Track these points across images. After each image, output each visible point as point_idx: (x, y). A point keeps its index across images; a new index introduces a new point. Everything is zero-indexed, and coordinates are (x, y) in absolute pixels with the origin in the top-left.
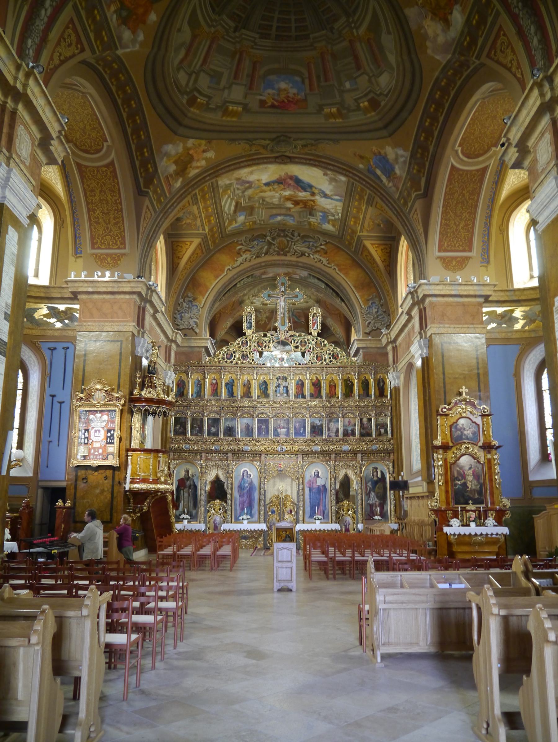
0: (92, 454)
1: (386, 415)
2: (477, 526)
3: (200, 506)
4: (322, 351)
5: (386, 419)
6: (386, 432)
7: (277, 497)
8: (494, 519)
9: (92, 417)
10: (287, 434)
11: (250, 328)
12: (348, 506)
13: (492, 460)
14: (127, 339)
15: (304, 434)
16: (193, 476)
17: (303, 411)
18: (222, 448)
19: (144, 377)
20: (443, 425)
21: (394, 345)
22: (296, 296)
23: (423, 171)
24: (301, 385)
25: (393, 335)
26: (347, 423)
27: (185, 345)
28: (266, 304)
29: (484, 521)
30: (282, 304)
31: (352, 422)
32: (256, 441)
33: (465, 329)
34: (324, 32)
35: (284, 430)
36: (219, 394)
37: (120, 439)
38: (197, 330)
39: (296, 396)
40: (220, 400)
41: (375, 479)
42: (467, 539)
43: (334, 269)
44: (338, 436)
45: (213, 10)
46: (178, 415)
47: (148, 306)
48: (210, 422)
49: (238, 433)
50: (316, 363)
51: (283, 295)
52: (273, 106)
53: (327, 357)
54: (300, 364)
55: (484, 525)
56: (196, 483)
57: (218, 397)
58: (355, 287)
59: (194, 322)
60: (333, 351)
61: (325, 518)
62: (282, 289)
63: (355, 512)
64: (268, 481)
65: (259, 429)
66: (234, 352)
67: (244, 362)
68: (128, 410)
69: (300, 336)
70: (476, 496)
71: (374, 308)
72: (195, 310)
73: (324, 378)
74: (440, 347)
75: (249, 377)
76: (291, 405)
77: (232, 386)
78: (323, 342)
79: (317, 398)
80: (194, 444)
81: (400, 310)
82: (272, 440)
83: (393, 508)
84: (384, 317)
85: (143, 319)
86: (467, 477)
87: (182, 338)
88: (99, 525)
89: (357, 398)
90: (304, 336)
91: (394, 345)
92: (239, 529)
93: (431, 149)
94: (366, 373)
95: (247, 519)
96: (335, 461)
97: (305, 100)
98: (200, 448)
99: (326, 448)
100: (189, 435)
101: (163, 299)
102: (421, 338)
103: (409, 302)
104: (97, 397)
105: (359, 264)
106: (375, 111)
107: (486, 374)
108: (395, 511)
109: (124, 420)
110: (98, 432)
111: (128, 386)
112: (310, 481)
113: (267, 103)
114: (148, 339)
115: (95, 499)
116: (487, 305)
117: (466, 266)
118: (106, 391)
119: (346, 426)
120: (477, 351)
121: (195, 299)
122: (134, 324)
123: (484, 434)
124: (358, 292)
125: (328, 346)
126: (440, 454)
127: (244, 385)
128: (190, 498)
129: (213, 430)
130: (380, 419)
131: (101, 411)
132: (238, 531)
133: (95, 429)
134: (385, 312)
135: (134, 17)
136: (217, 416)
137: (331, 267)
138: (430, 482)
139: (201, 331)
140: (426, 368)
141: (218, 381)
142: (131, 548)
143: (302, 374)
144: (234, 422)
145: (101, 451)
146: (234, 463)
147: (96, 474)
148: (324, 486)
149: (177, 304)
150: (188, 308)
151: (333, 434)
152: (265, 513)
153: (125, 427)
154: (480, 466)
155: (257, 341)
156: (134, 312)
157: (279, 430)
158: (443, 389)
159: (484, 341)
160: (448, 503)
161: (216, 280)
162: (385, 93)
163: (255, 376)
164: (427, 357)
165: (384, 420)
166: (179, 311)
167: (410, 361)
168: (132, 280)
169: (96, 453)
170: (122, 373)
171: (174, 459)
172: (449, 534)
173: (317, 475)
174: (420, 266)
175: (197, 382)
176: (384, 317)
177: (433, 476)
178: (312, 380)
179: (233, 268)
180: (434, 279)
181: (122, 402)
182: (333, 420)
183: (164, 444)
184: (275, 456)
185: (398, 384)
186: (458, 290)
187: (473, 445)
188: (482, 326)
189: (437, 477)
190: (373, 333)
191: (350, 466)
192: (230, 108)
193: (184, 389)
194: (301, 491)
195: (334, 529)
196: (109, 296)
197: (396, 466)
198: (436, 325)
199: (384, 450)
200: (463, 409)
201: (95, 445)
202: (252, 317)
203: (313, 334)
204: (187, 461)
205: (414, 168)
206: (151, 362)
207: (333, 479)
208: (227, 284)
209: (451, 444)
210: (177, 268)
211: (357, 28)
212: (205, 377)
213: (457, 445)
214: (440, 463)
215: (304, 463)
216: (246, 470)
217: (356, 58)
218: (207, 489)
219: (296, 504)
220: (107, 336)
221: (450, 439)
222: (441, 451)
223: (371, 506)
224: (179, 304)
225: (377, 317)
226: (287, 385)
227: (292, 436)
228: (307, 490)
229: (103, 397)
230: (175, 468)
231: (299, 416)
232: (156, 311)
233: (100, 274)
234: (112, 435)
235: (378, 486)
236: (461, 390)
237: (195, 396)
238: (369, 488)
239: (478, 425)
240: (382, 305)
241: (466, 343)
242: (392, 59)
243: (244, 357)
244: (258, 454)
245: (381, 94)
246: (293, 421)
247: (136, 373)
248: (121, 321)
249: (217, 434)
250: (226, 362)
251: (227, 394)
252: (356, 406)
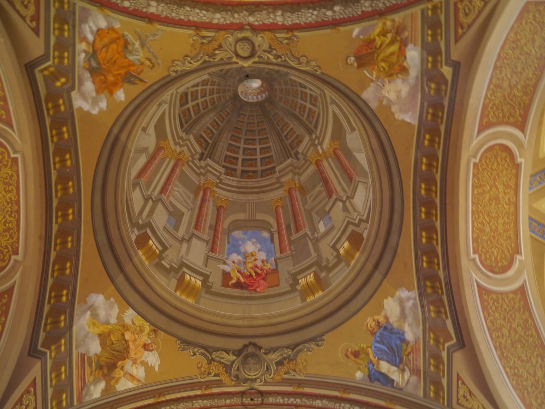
23: (443, 310)
34: (289, 161)
45: (182, 126)
52: (239, 285)
93: (441, 274)
97: (275, 271)
106: (358, 251)
113: (231, 278)
135: (103, 77)
162: (365, 218)
192: (187, 277)
205: (429, 310)
211: (321, 144)
217: (326, 182)
242: (362, 158)
245: (361, 220)
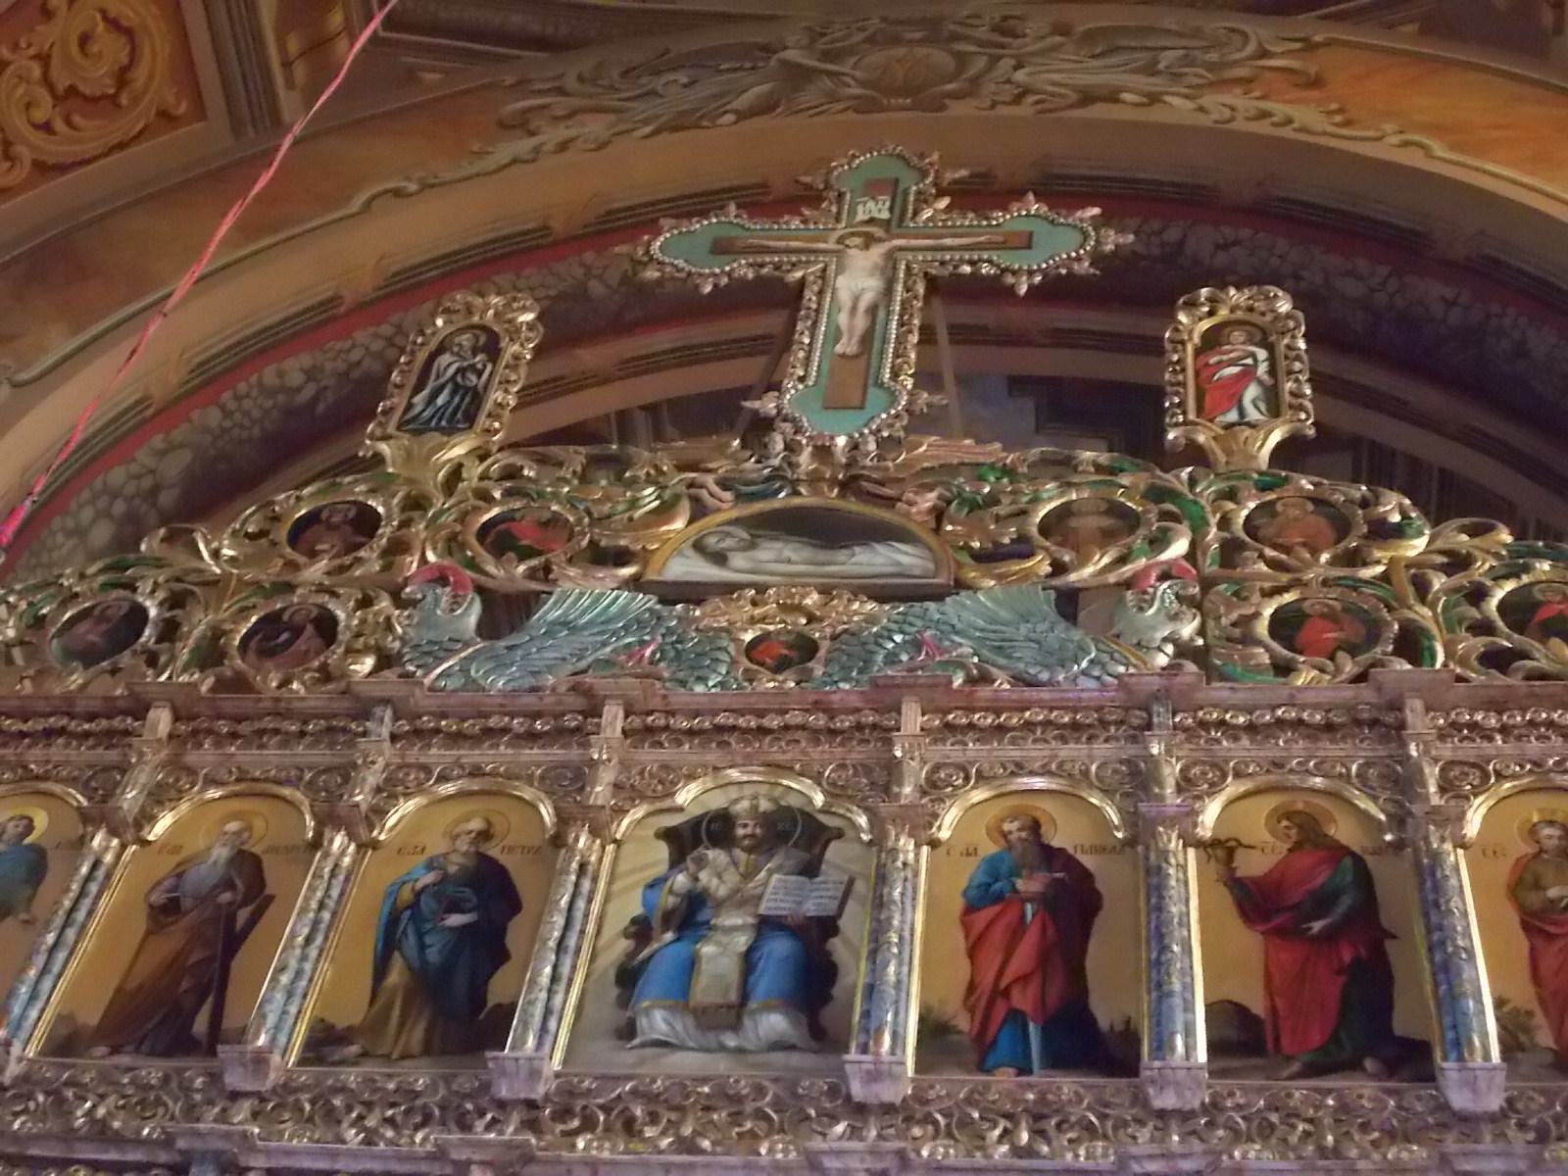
127: (165, 911)
178: (1221, 850)
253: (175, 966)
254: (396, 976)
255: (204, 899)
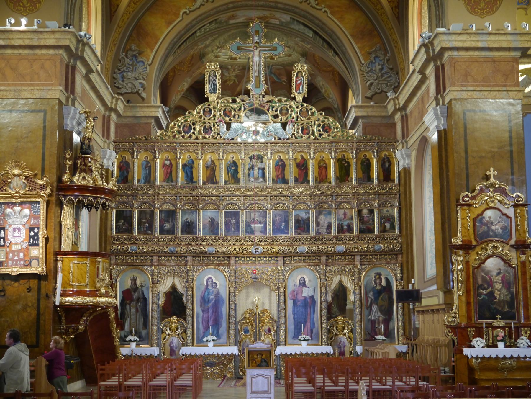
0: (10, 260)
1: (392, 206)
2: (506, 346)
3: (152, 325)
4: (309, 121)
5: (393, 210)
6: (393, 227)
7: (251, 312)
8: (528, 339)
9: (8, 210)
10: (264, 230)
11: (214, 91)
12: (343, 323)
13: (527, 263)
14: (52, 108)
15: (285, 230)
16: (142, 286)
17: (284, 200)
18: (179, 249)
19: (75, 159)
20: (464, 219)
21: (404, 113)
22: (275, 49)
24: (281, 166)
25: (402, 100)
26: (342, 216)
27: (129, 114)
28: (235, 59)
29: (516, 340)
30: (256, 59)
31: (349, 215)
32: (223, 240)
33: (495, 93)
35: (259, 225)
36: (174, 179)
37: (47, 240)
38: (144, 95)
39: (275, 181)
40: (176, 187)
41: (378, 287)
42: (493, 363)
43: (325, 11)
44: (330, 233)
46: (122, 207)
47: (79, 64)
48: (163, 215)
49: (199, 231)
50: (302, 137)
51: (257, 48)
53: (315, 130)
54: (280, 139)
55: (515, 345)
56: (146, 296)
57: (173, 184)
58: (352, 36)
59: (141, 83)
60: (323, 122)
61: (314, 339)
62: (256, 39)
63: (351, 331)
64: (240, 292)
65: (227, 225)
66: (194, 124)
67: (207, 136)
68: (56, 201)
69: (280, 101)
70: (506, 309)
71: (377, 64)
72: (141, 69)
73: (312, 156)
74: (462, 116)
75: (214, 157)
76: (269, 193)
77: (192, 168)
78: (311, 109)
79: (302, 183)
80: (142, 245)
81: (411, 68)
82: (245, 238)
83: (400, 324)
84: (390, 76)
85: (73, 82)
86: (495, 284)
87: (125, 106)
88: (23, 349)
89: (354, 183)
90: (286, 101)
91: (404, 113)
92: (202, 354)
94: (366, 151)
95: (213, 340)
96: (326, 265)
98: (150, 250)
99: (314, 248)
100: (136, 233)
101: (99, 54)
102: (437, 104)
103: (422, 56)
104: (15, 184)
105: (358, 6)
107: (522, 152)
108: (404, 329)
109: (51, 215)
110: (17, 231)
111: (55, 171)
112: (294, 291)
114: (79, 108)
115: (16, 317)
116: (526, 60)
117: (498, 8)
118: (26, 177)
119: (341, 220)
120: (510, 121)
121: (140, 53)
122: (61, 88)
123: (517, 230)
124: (356, 43)
125: (317, 114)
126: (460, 256)
127: (207, 167)
128: (138, 314)
129: (167, 226)
130: (385, 210)
131: (21, 204)
132: (201, 356)
133: (13, 226)
134: (391, 69)
136: (171, 207)
137: (321, 10)
138: (448, 292)
139: (149, 96)
140: (443, 144)
141: (173, 162)
142: (65, 378)
143: (283, 152)
144: (194, 216)
145: (21, 255)
146: (195, 269)
147: (16, 284)
148: (312, 297)
149: (117, 60)
150: (132, 65)
151: (323, 231)
152: (235, 333)
153: (52, 224)
154: (512, 270)
155: (223, 108)
156: (60, 71)
157: (253, 225)
158: (465, 171)
159: (519, 108)
160: (469, 318)
161: (168, 27)
163: (221, 154)
164: (444, 130)
165: (391, 211)
166: (119, 70)
167: (424, 134)
168: (57, 29)
169: (16, 258)
170: (47, 154)
171: (117, 265)
172: (470, 357)
173: (303, 284)
174: (437, 8)
175: (145, 163)
176: (390, 76)
177: (452, 283)
178: (295, 159)
179: (190, 12)
180: (455, 27)
181: (48, 191)
182: (324, 212)
183: (103, 245)
184: (248, 259)
185: (408, 164)
186: (487, 41)
187: (503, 245)
188: (517, 89)
189: (456, 284)
190: (377, 95)
191: (345, 271)
193: (128, 172)
194: (282, 305)
195: (324, 352)
196: (27, 52)
197: (405, 271)
198: (457, 88)
199: (390, 250)
200: (490, 197)
201: (14, 247)
202: (216, 76)
203: (297, 99)
204: (133, 266)
206: (84, 138)
207: (323, 288)
208: (183, 32)
209: (474, 243)
210: (116, 11)
212: (155, 156)
213: (482, 243)
214: (460, 267)
215: (286, 269)
216: (211, 278)
218: (160, 303)
219: (275, 321)
220: (25, 105)
221: (473, 236)
222: (461, 252)
223: (373, 322)
224: (120, 60)
225: (382, 76)
226: (263, 167)
227: (270, 233)
228: (290, 303)
229: (23, 185)
230: (118, 276)
231: (280, 207)
232: (90, 70)
233: (13, 21)
234: (36, 234)
235: (381, 297)
236: (488, 173)
237: (143, 181)
238: (370, 300)
239: (510, 218)
240: (388, 60)
241: (496, 111)
243: (207, 130)
244: (226, 257)
246: (271, 214)
247: (65, 154)
248: (43, 85)
249: (172, 231)
250: (183, 136)
251: (184, 178)
252: (353, 194)
253: (210, 174)
254: (230, 175)
255: (210, 166)
